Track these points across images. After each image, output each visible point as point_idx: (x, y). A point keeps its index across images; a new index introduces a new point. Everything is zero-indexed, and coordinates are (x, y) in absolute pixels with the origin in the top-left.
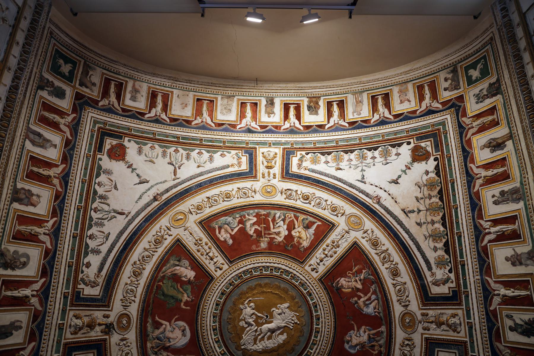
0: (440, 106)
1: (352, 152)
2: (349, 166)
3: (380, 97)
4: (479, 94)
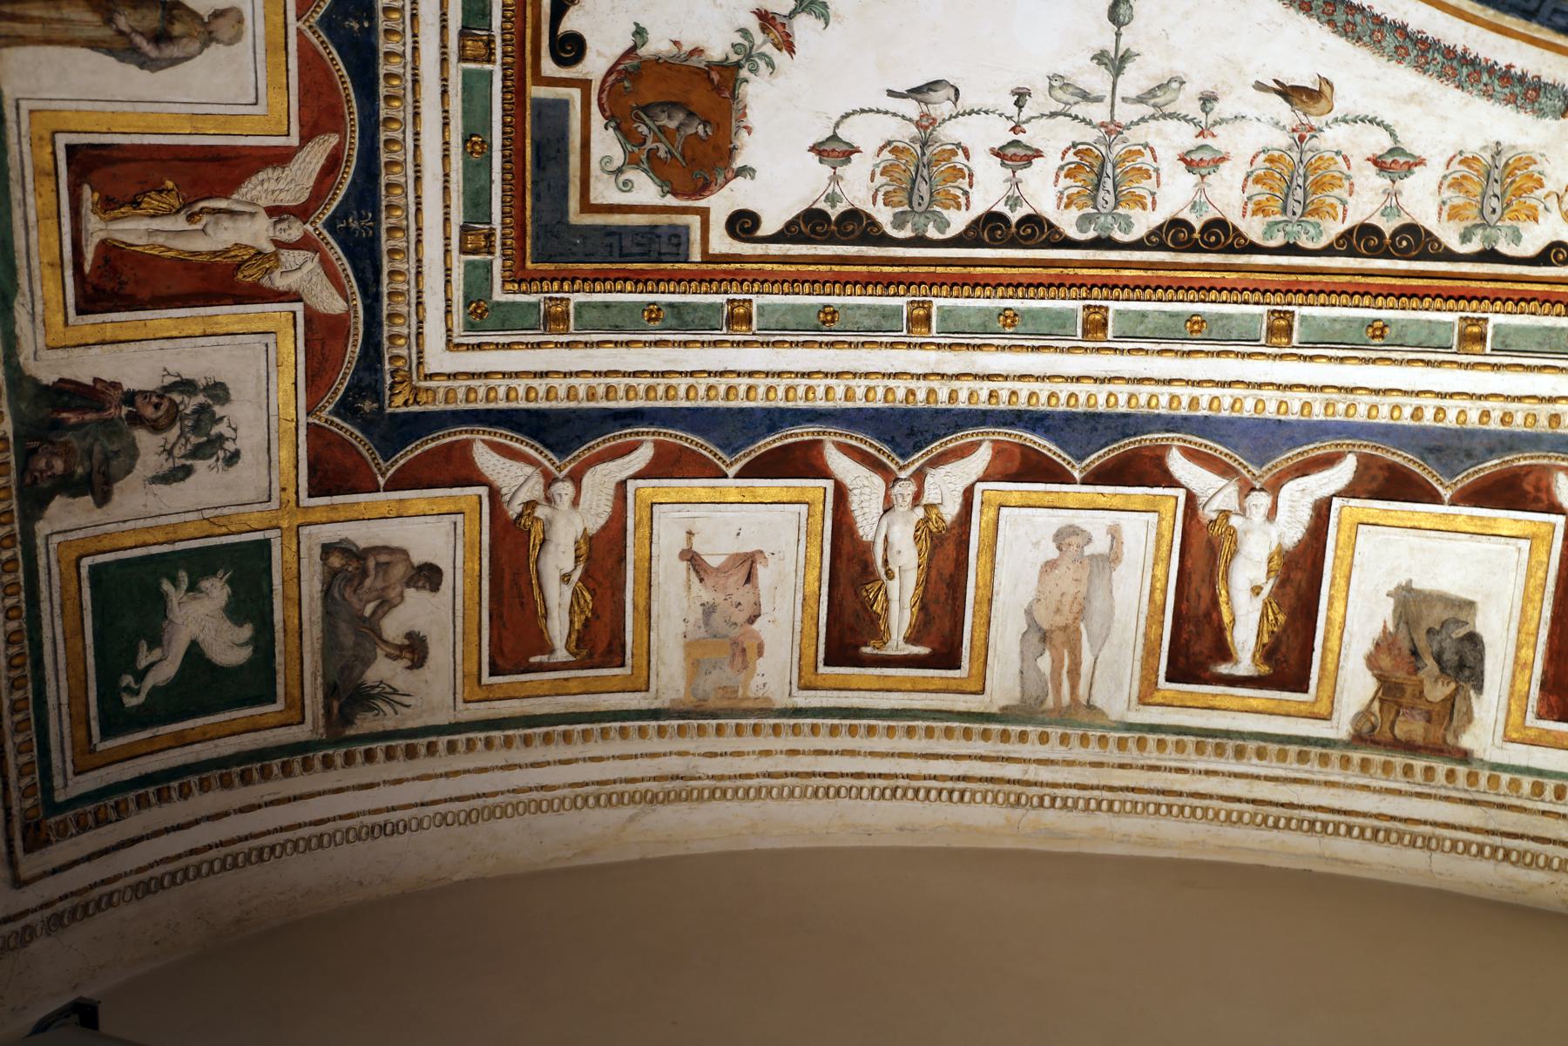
0: (486, 460)
1: (1174, 234)
2: (1222, 109)
3: (897, 644)
4: (197, 453)
